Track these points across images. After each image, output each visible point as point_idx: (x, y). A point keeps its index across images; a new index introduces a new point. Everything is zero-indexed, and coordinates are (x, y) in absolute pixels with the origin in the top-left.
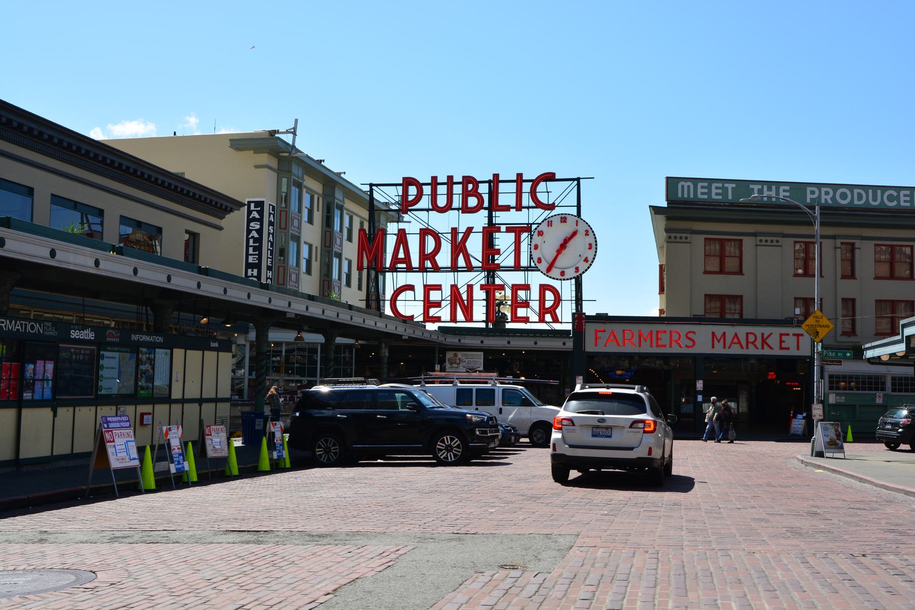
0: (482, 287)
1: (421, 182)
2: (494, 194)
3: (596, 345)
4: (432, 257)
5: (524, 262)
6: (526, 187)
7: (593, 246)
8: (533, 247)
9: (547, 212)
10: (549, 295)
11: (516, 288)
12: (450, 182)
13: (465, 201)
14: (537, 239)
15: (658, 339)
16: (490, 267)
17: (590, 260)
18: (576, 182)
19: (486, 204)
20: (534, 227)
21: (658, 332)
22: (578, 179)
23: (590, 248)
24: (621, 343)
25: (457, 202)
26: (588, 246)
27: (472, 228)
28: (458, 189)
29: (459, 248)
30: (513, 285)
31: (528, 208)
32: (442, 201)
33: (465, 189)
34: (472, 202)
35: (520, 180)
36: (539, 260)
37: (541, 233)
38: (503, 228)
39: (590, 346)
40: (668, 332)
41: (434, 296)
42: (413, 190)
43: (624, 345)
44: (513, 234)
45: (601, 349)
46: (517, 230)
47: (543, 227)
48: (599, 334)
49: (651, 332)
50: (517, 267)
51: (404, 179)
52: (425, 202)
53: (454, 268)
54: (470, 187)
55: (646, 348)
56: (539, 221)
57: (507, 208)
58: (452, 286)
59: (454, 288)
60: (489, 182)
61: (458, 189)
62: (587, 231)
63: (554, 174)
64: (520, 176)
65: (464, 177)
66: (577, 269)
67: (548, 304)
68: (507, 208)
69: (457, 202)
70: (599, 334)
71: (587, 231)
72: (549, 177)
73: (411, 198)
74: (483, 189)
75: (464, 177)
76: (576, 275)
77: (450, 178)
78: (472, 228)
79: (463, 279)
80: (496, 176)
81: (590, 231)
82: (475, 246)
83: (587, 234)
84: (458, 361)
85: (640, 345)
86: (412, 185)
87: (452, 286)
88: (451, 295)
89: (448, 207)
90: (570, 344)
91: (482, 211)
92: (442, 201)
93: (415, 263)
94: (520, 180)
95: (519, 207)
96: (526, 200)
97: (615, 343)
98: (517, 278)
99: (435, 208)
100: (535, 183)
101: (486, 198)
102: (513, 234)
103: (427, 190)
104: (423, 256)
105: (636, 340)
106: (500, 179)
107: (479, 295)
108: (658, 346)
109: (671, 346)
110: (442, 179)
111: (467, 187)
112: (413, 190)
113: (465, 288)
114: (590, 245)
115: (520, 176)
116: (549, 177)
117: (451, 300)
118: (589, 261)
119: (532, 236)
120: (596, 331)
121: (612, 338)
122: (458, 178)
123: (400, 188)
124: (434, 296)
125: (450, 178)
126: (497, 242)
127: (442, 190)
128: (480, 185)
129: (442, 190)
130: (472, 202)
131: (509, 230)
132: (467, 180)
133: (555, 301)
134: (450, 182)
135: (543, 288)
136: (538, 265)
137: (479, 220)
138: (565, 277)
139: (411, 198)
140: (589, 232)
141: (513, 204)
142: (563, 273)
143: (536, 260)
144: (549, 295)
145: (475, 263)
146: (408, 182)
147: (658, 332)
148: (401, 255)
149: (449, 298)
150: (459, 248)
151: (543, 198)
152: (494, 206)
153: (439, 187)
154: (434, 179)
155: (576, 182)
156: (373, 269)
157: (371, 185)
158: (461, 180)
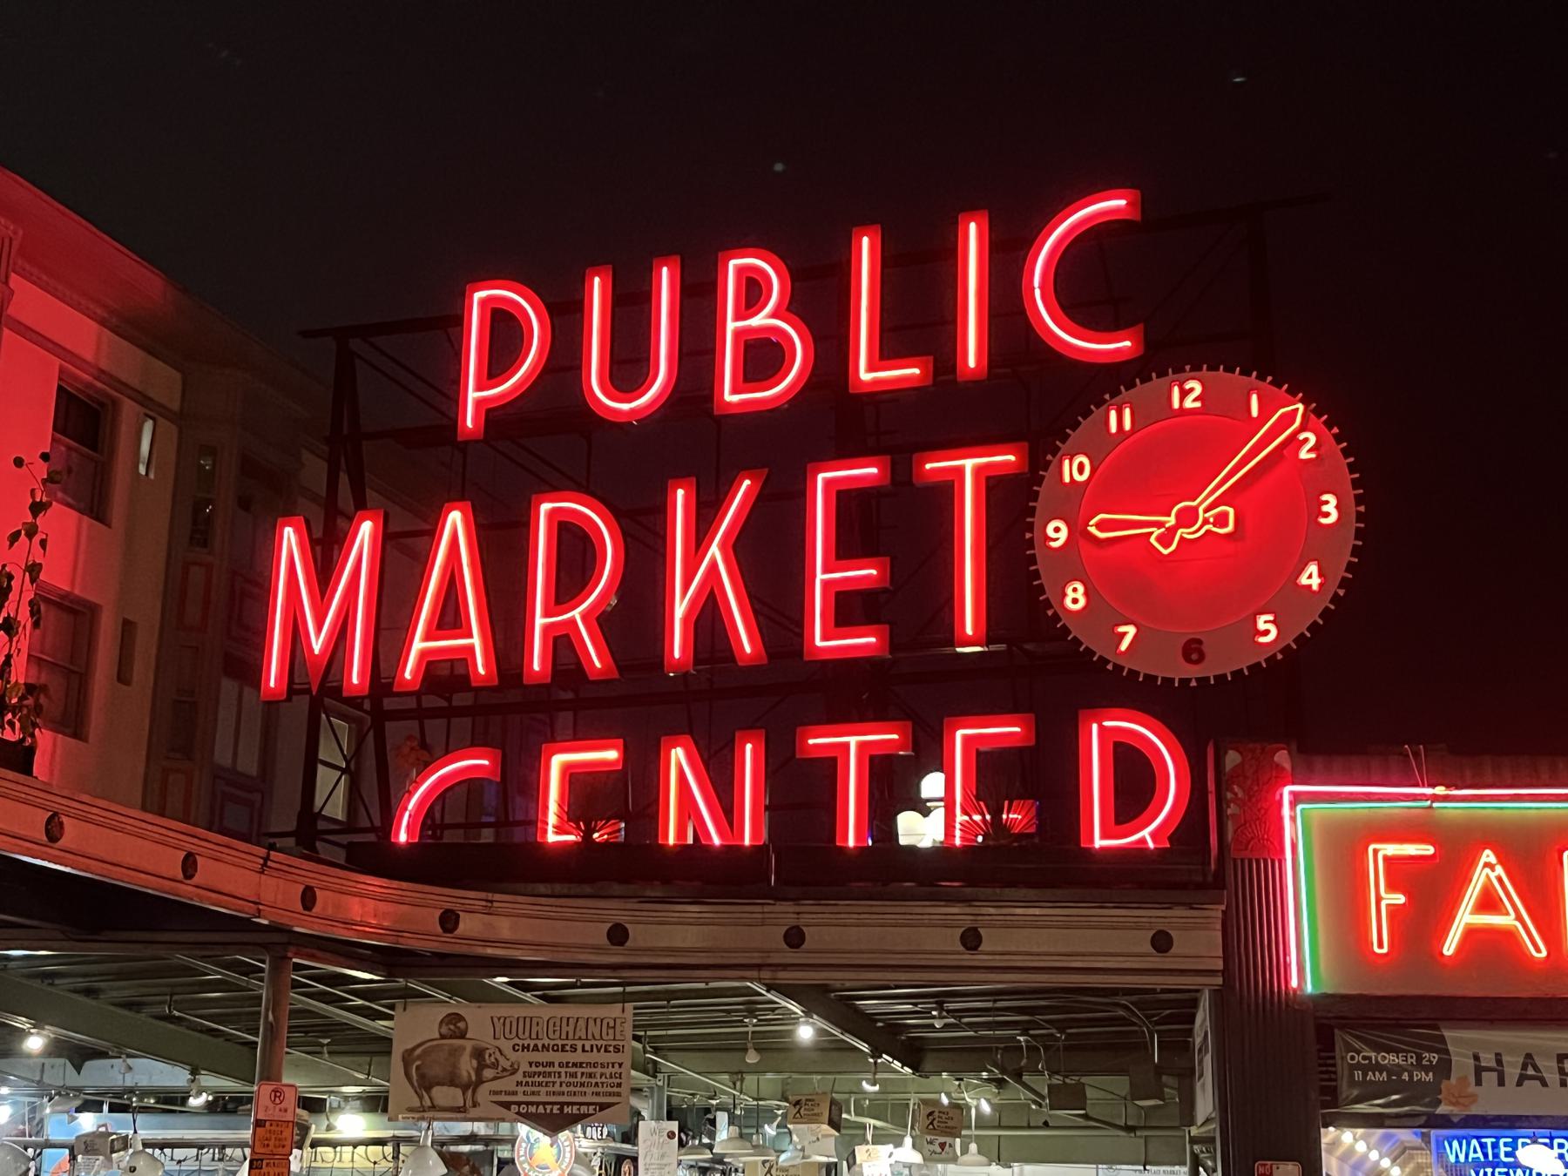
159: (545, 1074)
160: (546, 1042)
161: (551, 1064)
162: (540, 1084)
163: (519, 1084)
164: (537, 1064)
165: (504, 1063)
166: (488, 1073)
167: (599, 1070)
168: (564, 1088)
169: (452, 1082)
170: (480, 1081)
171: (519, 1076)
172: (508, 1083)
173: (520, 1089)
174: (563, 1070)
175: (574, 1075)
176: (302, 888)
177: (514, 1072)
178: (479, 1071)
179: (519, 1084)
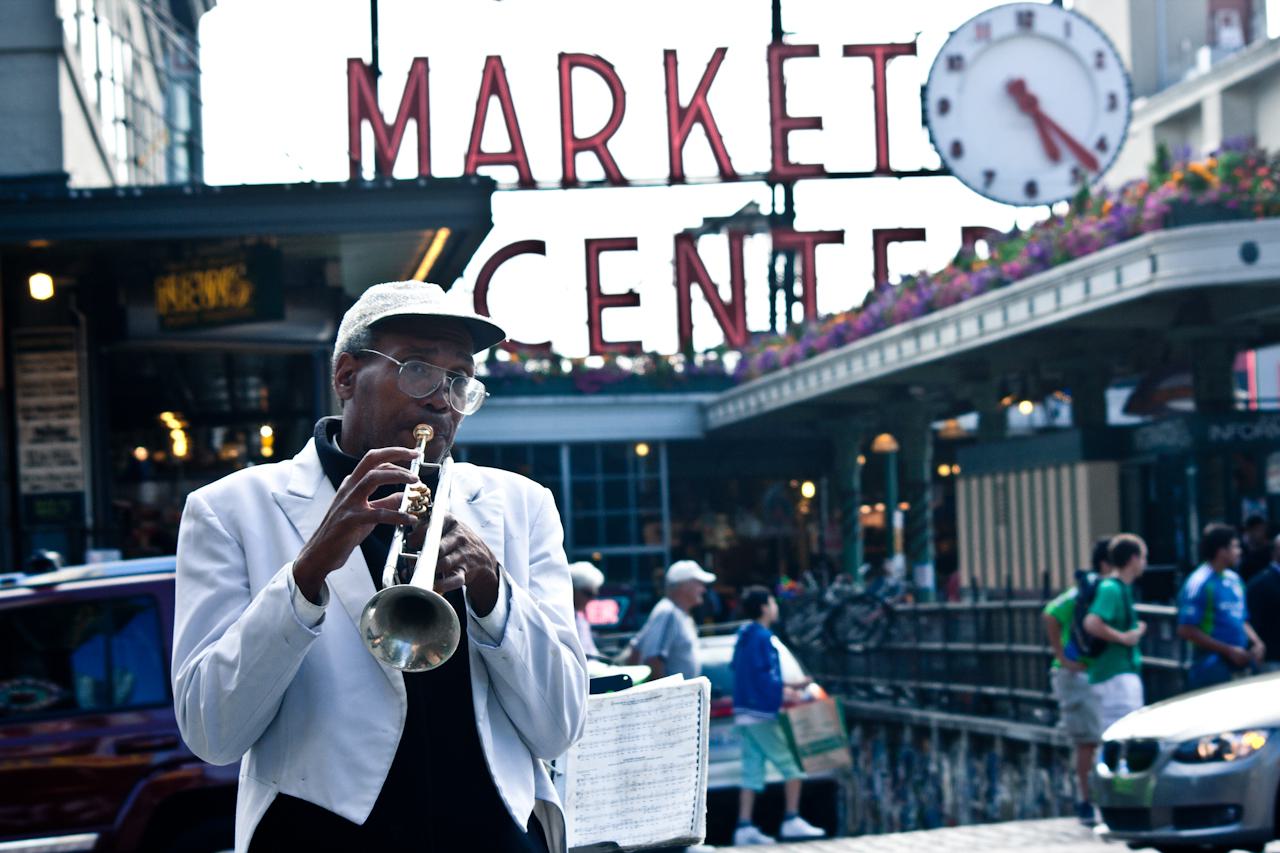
4: (598, 145)
26: (1104, 102)
29: (686, 116)
36: (957, 149)
37: (955, 63)
38: (831, 50)
41: (615, 273)
62: (1100, 55)
71: (1100, 55)
81: (1109, 59)
93: (546, 162)
104: (572, 146)
124: (615, 273)
136: (953, 164)
143: (946, 148)
148: (496, 140)
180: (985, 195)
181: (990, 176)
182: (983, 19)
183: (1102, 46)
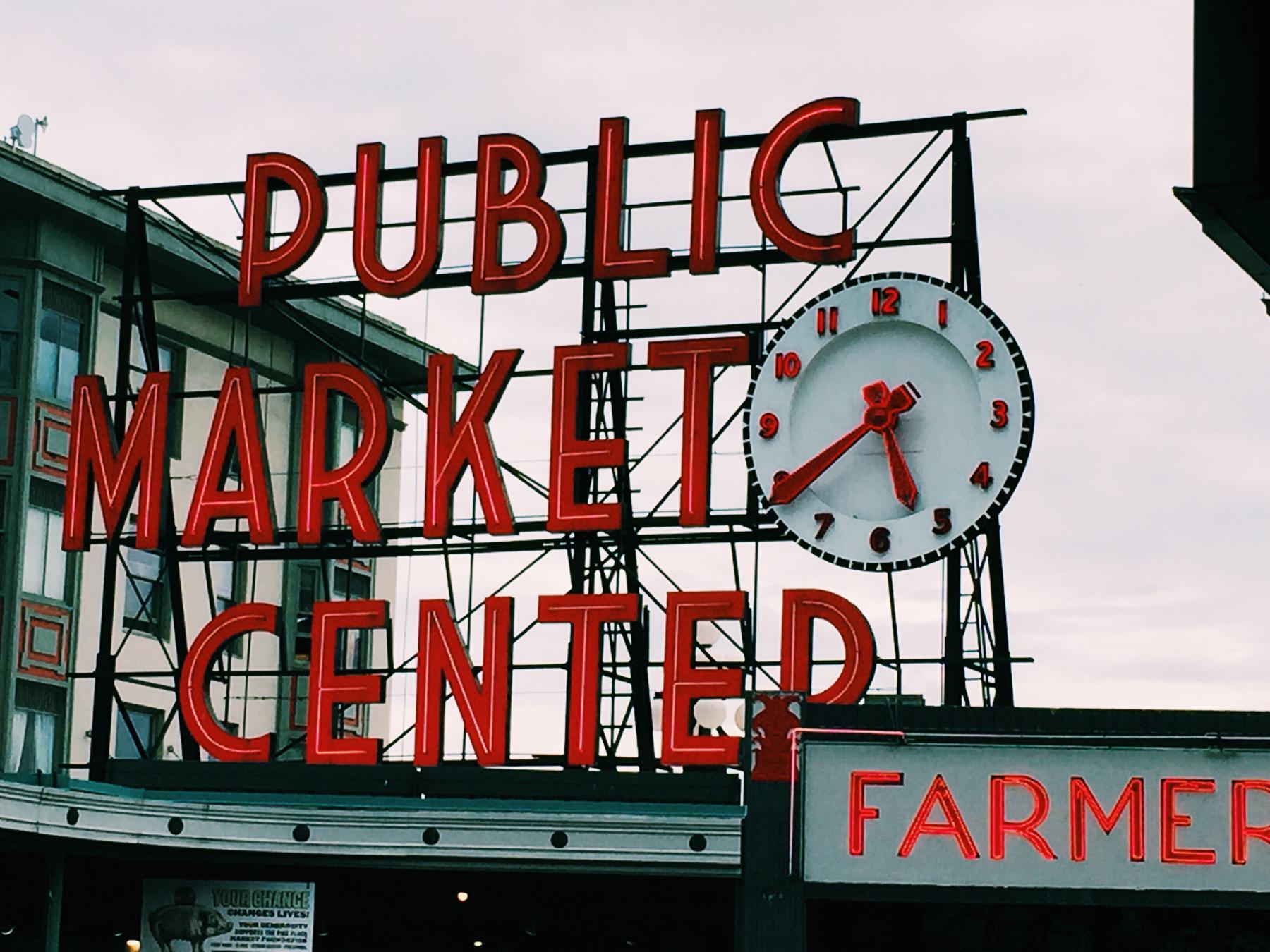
0: (549, 610)
1: (321, 171)
2: (606, 204)
3: (857, 846)
5: (728, 495)
6: (737, 169)
7: (1018, 417)
8: (755, 427)
9: (832, 275)
10: (827, 640)
11: (690, 609)
12: (433, 163)
13: (488, 243)
14: (774, 395)
15: (1170, 821)
16: (596, 526)
17: (1000, 474)
18: (947, 137)
19: (575, 251)
20: (769, 335)
21: (1169, 787)
22: (957, 122)
23: (1000, 423)
24: (981, 837)
25: (458, 250)
27: (519, 353)
28: (460, 194)
30: (677, 598)
31: (757, 259)
32: (397, 250)
33: (489, 193)
34: (519, 242)
35: (710, 137)
37: (788, 367)
38: (640, 350)
39: (827, 860)
40: (1223, 788)
42: (285, 211)
43: (998, 849)
44: (674, 379)
45: (879, 867)
46: (696, 355)
47: (802, 341)
48: (873, 796)
49: (1136, 787)
50: (696, 518)
51: (252, 159)
52: (332, 261)
53: (440, 530)
54: (511, 178)
55: (1109, 867)
56: (786, 314)
57: (660, 263)
58: (426, 606)
59: (437, 616)
60: (589, 155)
61: (460, 194)
63: (852, 105)
64: (711, 119)
65: (484, 140)
66: (943, 517)
67: (823, 680)
68: (660, 263)
69: (458, 250)
70: (873, 796)
72: (834, 121)
73: (275, 243)
74: (566, 188)
75: (484, 140)
76: (936, 545)
77: (433, 146)
78: (519, 353)
79: (491, 572)
80: (615, 127)
81: (1002, 356)
82: (523, 429)
83: (986, 361)
84: (195, 926)
85: (1078, 851)
86: (284, 186)
87: (426, 606)
88: (420, 655)
89: (425, 274)
90: (725, 850)
91: (551, 284)
92: (397, 250)
94: (710, 137)
95: (707, 257)
96: (740, 228)
97: (952, 841)
98: (699, 567)
99: (371, 276)
100: (773, 149)
101: (576, 228)
102: (674, 379)
103: (341, 203)
105: (1056, 828)
106: (634, 139)
107: (544, 644)
108: (1170, 854)
109: (1238, 856)
110: (401, 155)
111: (498, 182)
112: (285, 211)
113: (479, 618)
114: (1001, 408)
115: (711, 119)
116: (834, 121)
117: (419, 671)
118: (998, 485)
119: (755, 374)
120: (859, 782)
121: (937, 816)
122: (461, 150)
123: (239, 198)
125: (433, 146)
126: (633, 414)
127: (399, 200)
128: (554, 172)
129: (399, 200)
130: (519, 242)
131: (661, 359)
132: (503, 152)
133: (848, 663)
134: (433, 163)
135: (804, 607)
137: (548, 319)
138: (893, 557)
139: (275, 243)
140: (1000, 349)
141: (680, 244)
142: (880, 540)
144: (827, 640)
145: (528, 504)
146: (270, 173)
147: (1169, 787)
149: (413, 664)
150: (462, 449)
151: (814, 217)
152: (611, 262)
153: (389, 188)
154: (371, 152)
155: (947, 137)
156: (130, 542)
157: (135, 194)
158: (473, 156)
159: (252, 932)
160: (252, 908)
161: (256, 925)
162: (248, 939)
163: (232, 938)
164: (246, 925)
165: (221, 923)
166: (210, 930)
167: (290, 930)
168: (265, 942)
169: (185, 936)
170: (205, 936)
171: (232, 933)
172: (224, 938)
173: (234, 943)
174: (264, 930)
175: (272, 933)
176: (67, 810)
177: (229, 930)
178: (204, 928)
179: (232, 938)
180: (816, 552)
181: (826, 521)
182: (827, 304)
183: (994, 337)
